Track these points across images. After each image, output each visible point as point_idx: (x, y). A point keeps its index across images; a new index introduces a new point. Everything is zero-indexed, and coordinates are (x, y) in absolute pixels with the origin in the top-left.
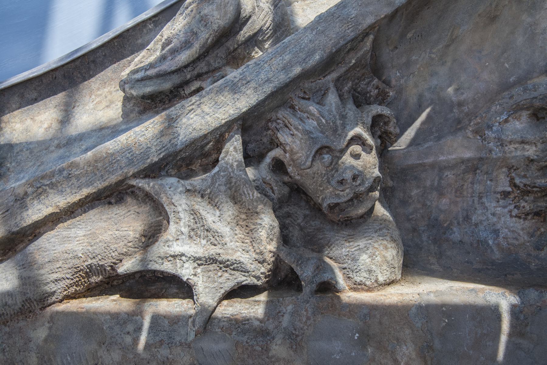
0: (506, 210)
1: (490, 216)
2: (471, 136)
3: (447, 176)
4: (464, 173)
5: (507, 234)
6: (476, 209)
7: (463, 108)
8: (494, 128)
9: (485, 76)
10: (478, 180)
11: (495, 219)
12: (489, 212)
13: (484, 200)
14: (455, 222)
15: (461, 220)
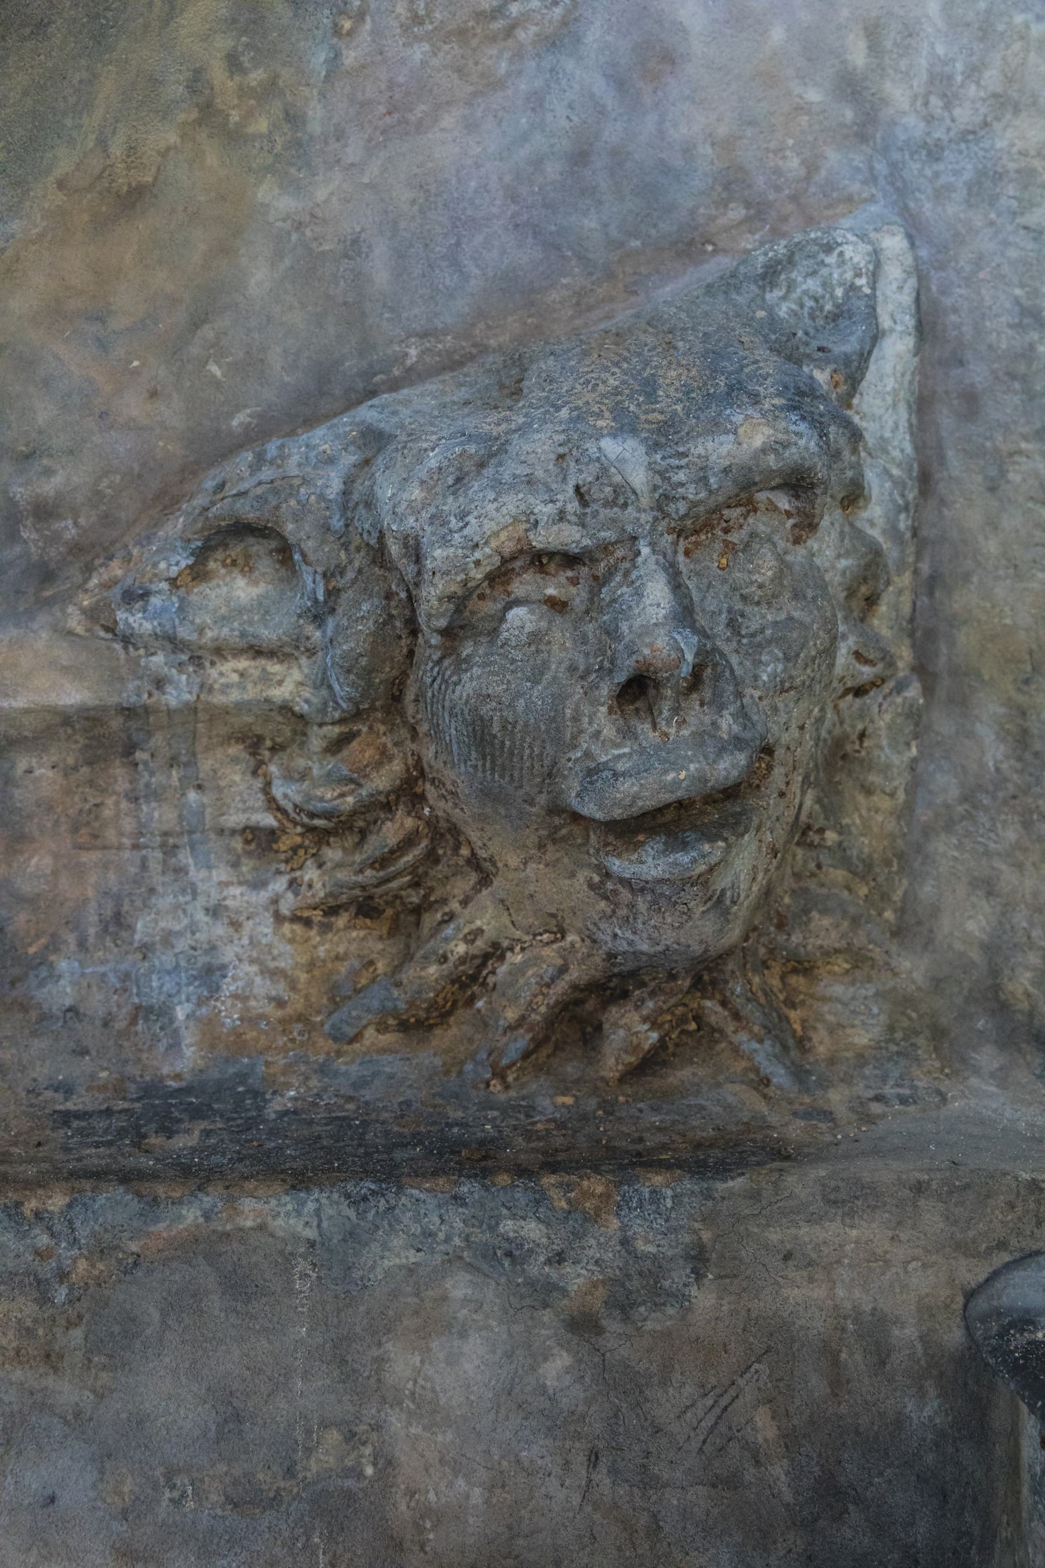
0: (263, 896)
1: (201, 917)
2: (80, 630)
3: (30, 771)
4: (90, 764)
5: (250, 984)
6: (152, 891)
7: (58, 525)
8: (155, 601)
9: (133, 405)
10: (147, 785)
11: (220, 930)
12: (201, 901)
13: (185, 857)
14: (71, 939)
15: (92, 931)
